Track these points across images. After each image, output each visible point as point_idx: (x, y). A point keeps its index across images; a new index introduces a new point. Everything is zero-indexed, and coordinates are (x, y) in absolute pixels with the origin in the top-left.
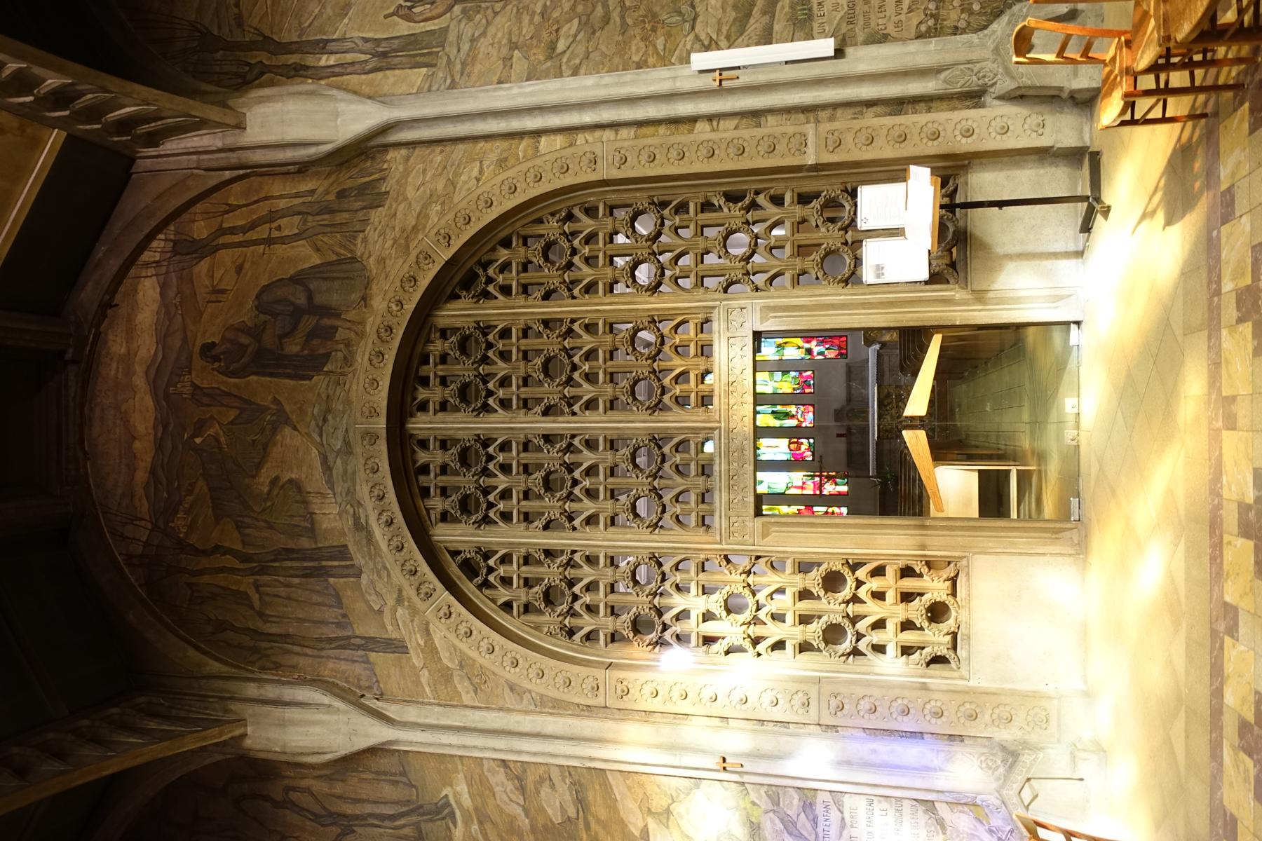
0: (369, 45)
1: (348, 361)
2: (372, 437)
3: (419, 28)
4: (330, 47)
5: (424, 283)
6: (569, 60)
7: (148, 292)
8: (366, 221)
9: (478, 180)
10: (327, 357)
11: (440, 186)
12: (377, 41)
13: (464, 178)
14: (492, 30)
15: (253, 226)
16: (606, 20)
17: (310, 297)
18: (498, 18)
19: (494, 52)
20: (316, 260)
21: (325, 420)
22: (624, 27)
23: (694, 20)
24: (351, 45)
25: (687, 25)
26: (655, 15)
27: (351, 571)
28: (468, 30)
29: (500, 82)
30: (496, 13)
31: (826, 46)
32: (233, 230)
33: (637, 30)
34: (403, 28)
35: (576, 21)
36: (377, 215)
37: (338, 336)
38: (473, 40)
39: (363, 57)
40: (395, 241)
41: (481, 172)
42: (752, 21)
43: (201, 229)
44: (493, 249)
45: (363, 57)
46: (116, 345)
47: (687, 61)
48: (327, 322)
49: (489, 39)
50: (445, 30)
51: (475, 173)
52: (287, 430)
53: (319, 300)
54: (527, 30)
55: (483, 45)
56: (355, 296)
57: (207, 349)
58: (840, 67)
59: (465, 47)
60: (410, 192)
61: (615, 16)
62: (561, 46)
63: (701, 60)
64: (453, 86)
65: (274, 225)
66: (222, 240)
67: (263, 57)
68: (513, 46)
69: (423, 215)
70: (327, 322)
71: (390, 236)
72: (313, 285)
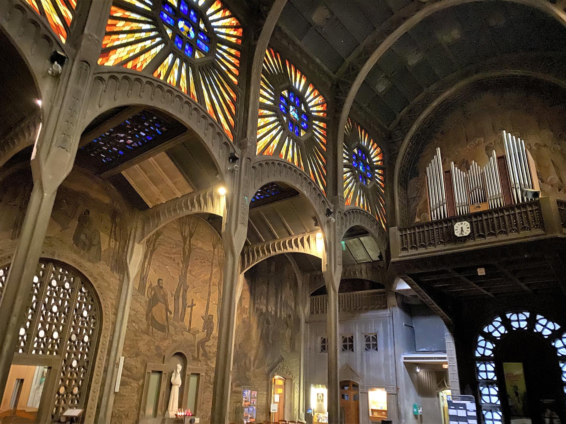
0: (146, 275)
1: (75, 252)
2: (53, 254)
3: (146, 289)
4: (149, 266)
5: (90, 279)
6: (130, 325)
7: (107, 200)
8: (108, 266)
9: (110, 297)
10: (77, 246)
11: (111, 287)
12: (146, 278)
13: (111, 294)
14: (141, 307)
15: (115, 234)
16: (136, 336)
17: (94, 245)
18: (143, 309)
19: (137, 307)
20: (103, 250)
21: (61, 241)
22: (133, 340)
23: (131, 358)
24: (148, 271)
25: (129, 355)
26: (134, 348)
27: (14, 237)
28: (143, 301)
29: (130, 307)
30: (144, 309)
31: (117, 390)
32: (115, 228)
33: (132, 343)
34: (147, 285)
35: (138, 328)
36: (109, 268)
37: (82, 250)
38: (140, 302)
39: (144, 274)
40: (102, 272)
41: (112, 299)
42: (126, 371)
43: (118, 220)
44: (91, 297)
45: (144, 274)
46: (96, 187)
47: (123, 355)
48: (87, 248)
49: (140, 306)
50: (144, 295)
51: (112, 297)
52: (60, 229)
53: (93, 248)
54: (138, 316)
55: (139, 305)
56: (91, 258)
57: (88, 212)
58: (112, 393)
59: (139, 300)
60: (112, 279)
61: (136, 338)
62: (134, 324)
63: (122, 358)
64: (133, 295)
65: (114, 240)
66: (114, 225)
67: (151, 248)
68: (137, 312)
69: (106, 281)
70: (87, 248)
71: (103, 271)
72: (97, 247)
